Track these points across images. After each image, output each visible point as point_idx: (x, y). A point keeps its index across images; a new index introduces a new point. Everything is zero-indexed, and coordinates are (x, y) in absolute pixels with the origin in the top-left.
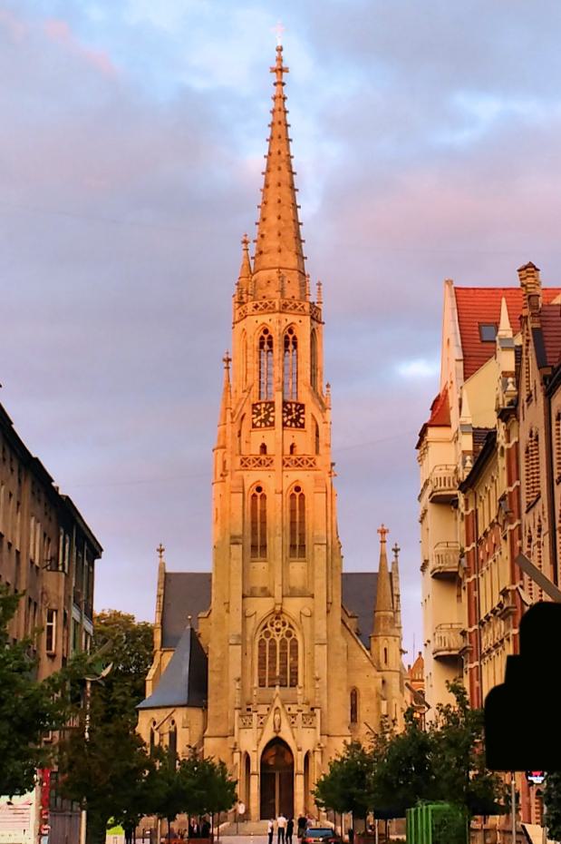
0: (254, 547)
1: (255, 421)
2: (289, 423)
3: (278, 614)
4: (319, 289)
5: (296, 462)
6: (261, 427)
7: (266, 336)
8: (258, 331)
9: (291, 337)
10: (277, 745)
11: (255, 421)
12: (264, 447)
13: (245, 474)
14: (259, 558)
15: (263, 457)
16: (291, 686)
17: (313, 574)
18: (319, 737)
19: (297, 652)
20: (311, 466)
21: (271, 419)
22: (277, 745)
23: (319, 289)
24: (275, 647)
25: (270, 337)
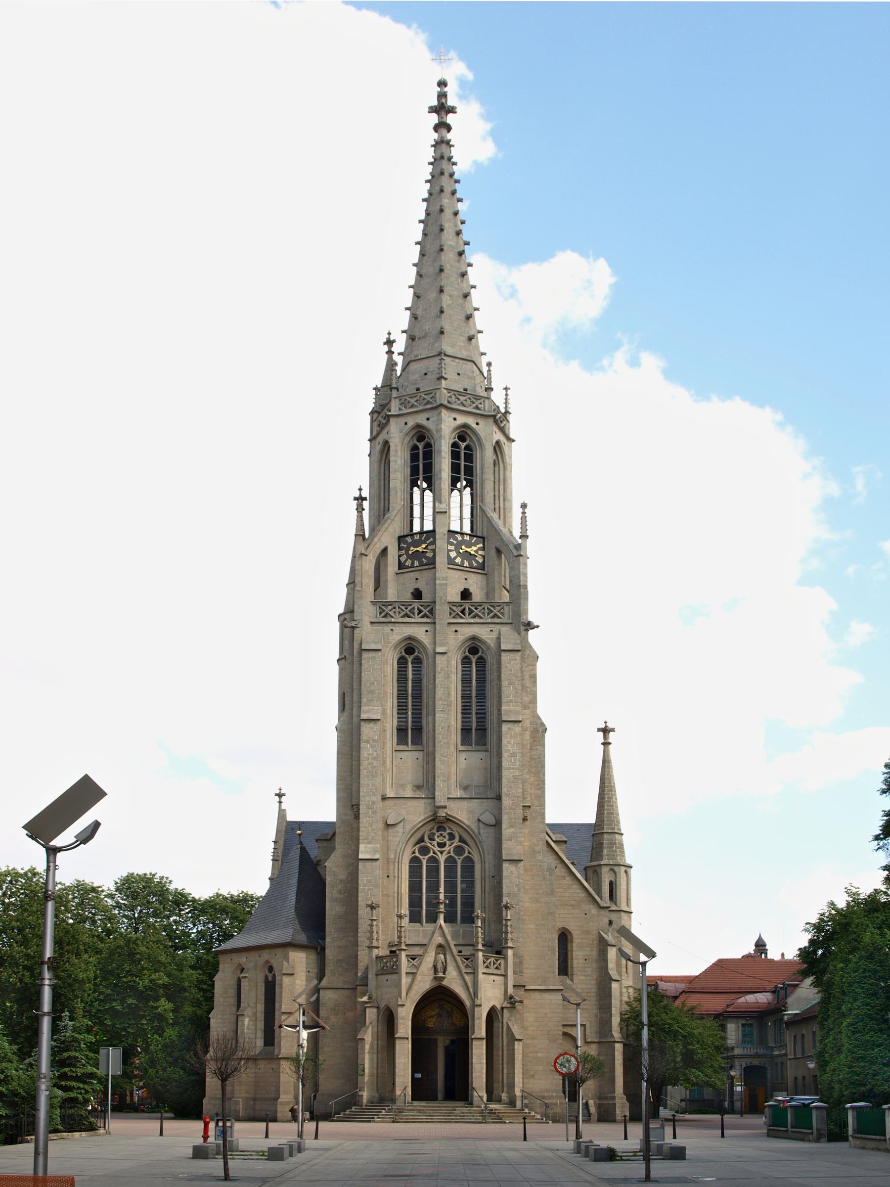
0: (401, 732)
1: (403, 559)
2: (458, 560)
4: (507, 395)
5: (471, 611)
6: (413, 566)
7: (421, 446)
8: (407, 439)
9: (463, 445)
10: (442, 1007)
11: (403, 559)
12: (417, 594)
13: (387, 629)
15: (416, 605)
17: (500, 762)
18: (511, 990)
19: (473, 876)
20: (495, 616)
21: (430, 555)
22: (439, 999)
23: (507, 395)
24: (437, 869)
25: (429, 445)
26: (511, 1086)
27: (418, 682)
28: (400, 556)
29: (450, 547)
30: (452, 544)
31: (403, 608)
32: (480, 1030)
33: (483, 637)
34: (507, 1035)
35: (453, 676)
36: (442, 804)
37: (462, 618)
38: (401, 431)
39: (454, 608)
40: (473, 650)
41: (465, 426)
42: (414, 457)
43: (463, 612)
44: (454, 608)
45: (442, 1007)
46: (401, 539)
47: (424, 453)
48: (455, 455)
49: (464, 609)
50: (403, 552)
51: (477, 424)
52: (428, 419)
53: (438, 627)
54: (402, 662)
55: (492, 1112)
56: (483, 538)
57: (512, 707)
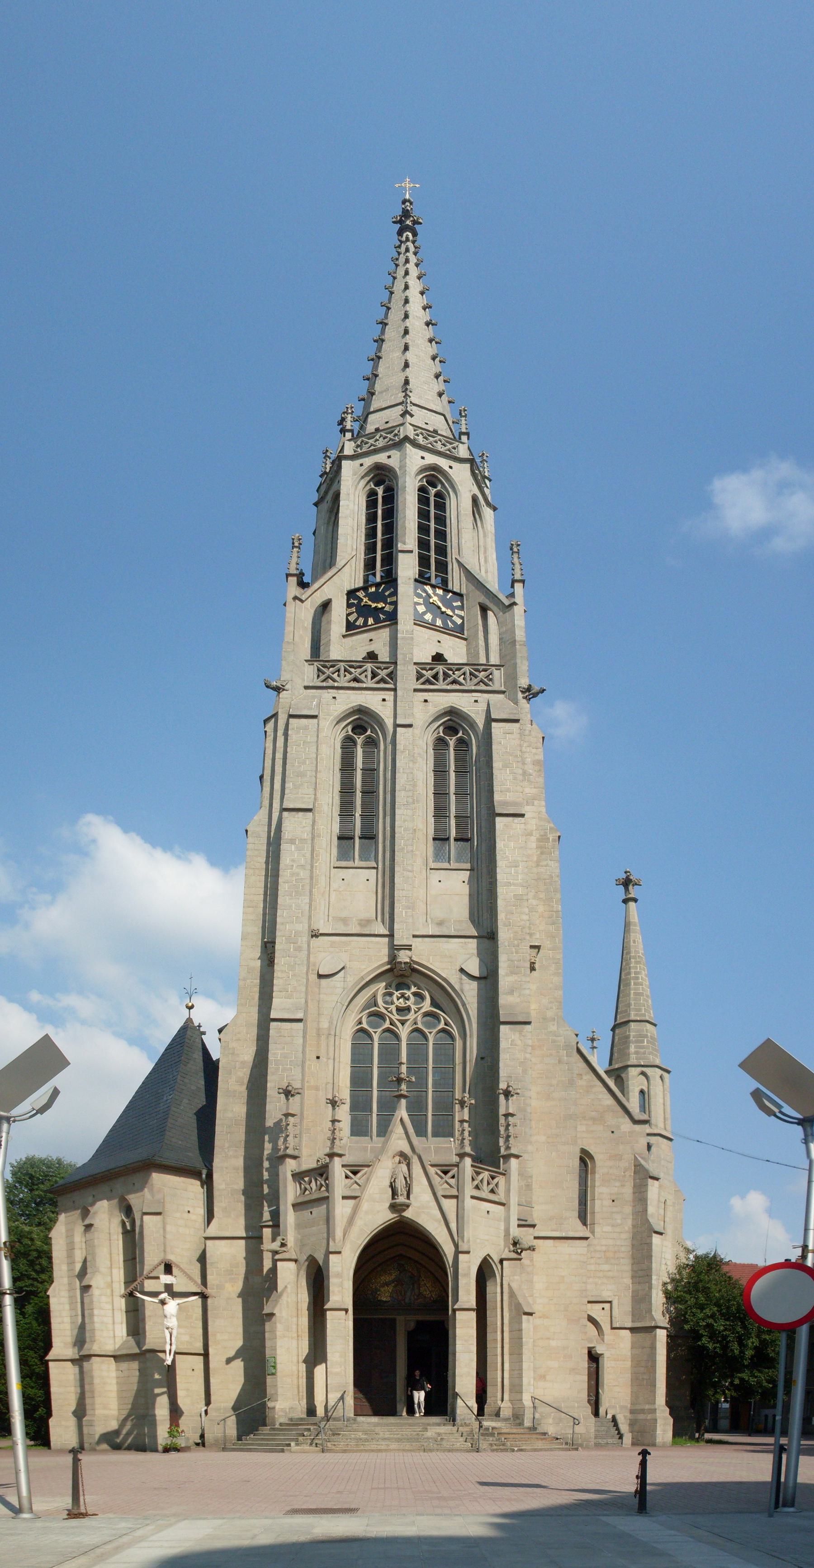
0: (345, 838)
3: (400, 974)
7: (380, 491)
8: (363, 482)
9: (433, 491)
12: (372, 656)
13: (327, 695)
14: (357, 863)
15: (369, 666)
16: (435, 1134)
21: (388, 608)
26: (517, 1388)
27: (370, 772)
28: (348, 615)
29: (416, 600)
30: (419, 596)
31: (352, 670)
32: (467, 1295)
33: (465, 710)
34: (510, 1305)
35: (421, 762)
36: (405, 942)
37: (431, 683)
38: (354, 474)
39: (424, 672)
40: (451, 729)
41: (435, 468)
42: (371, 503)
43: (435, 677)
44: (424, 672)
45: (403, 1261)
46: (351, 594)
47: (383, 497)
48: (423, 500)
49: (437, 673)
50: (354, 609)
51: (451, 467)
52: (389, 457)
53: (399, 693)
54: (348, 744)
55: (487, 1433)
56: (460, 595)
57: (509, 797)
